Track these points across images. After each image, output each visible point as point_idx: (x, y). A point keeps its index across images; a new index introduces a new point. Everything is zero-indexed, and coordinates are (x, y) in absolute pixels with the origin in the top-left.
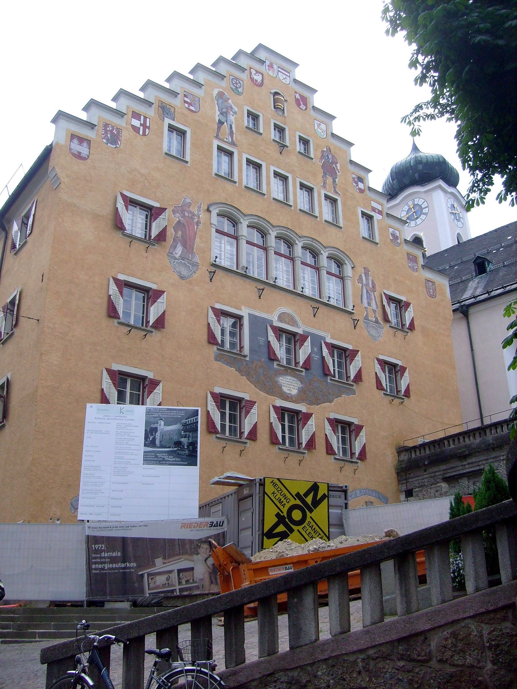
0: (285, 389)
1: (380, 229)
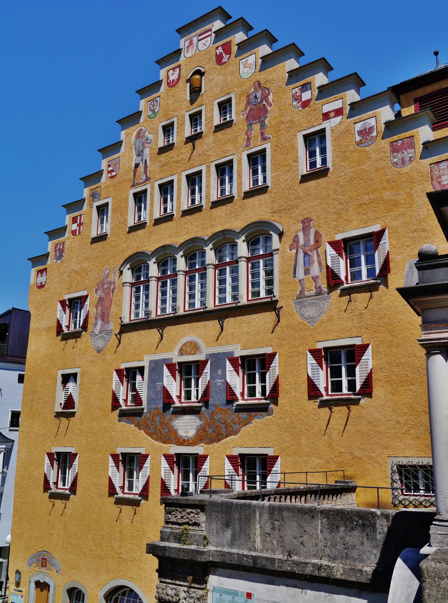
0: (181, 433)
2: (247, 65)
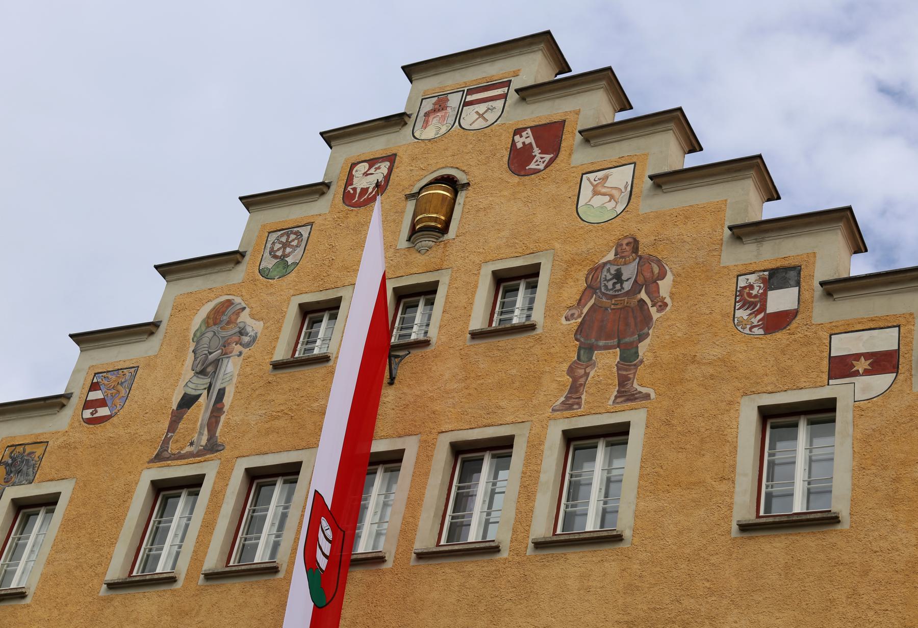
2: (604, 190)
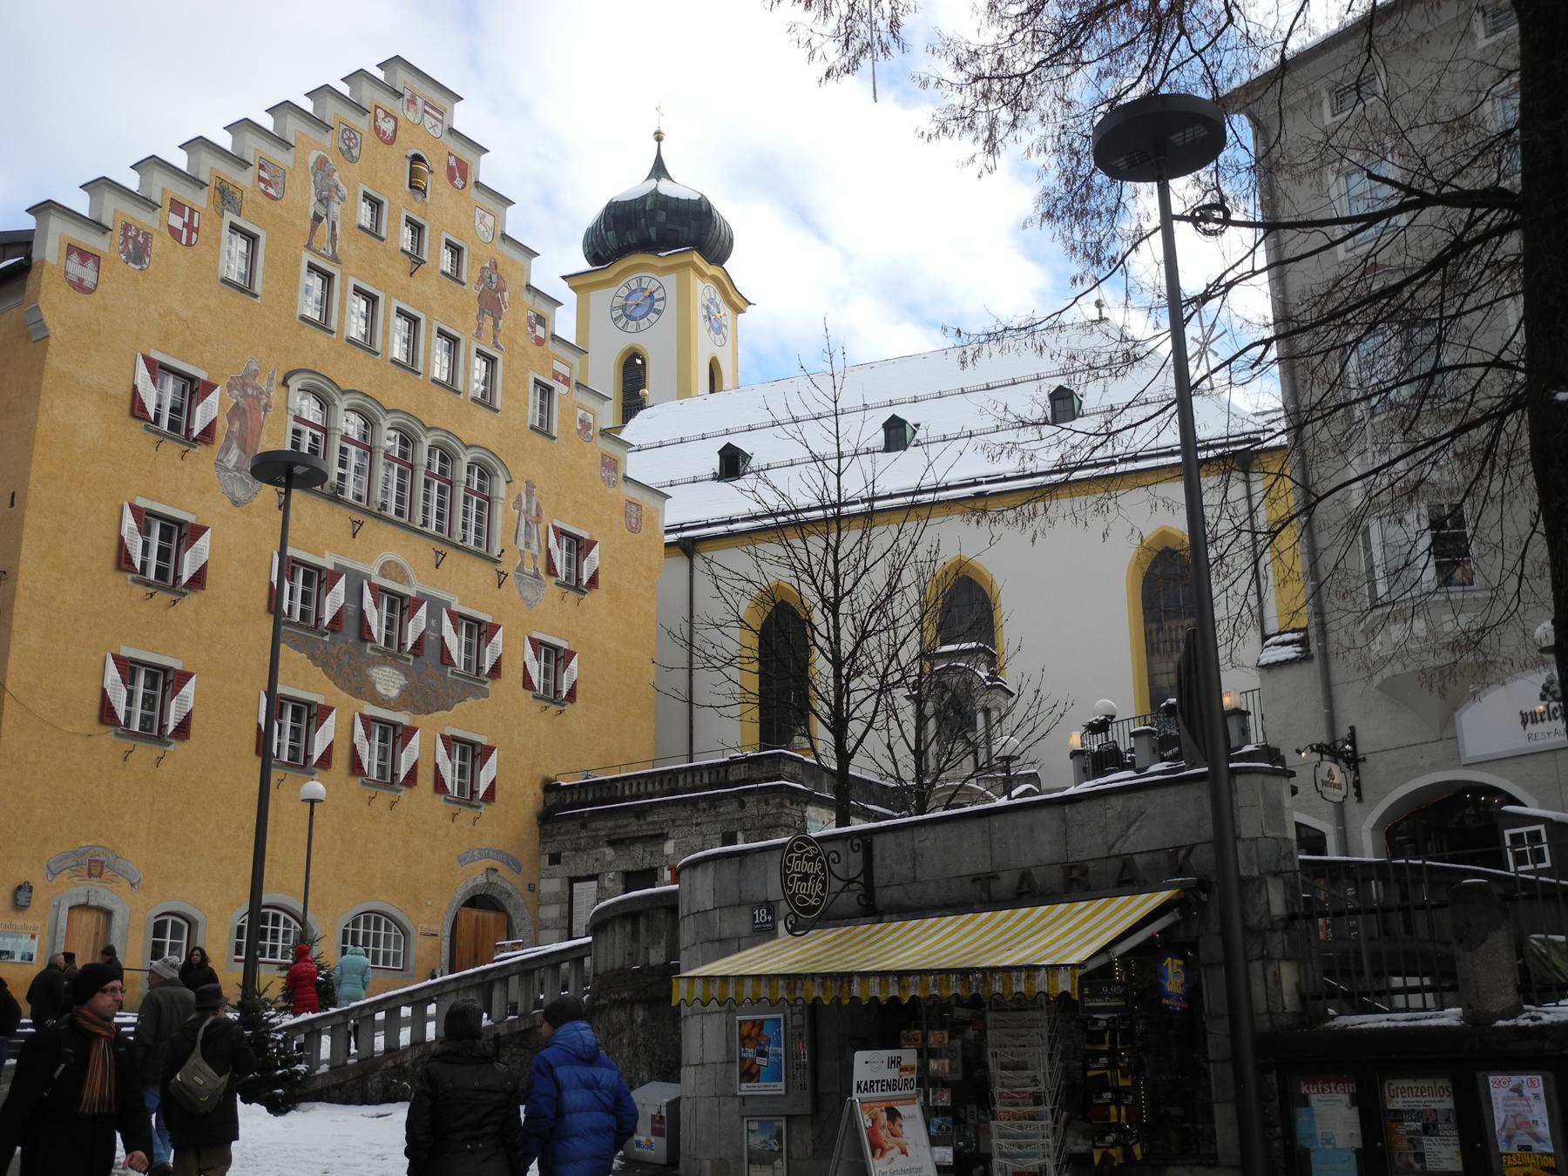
0: (380, 688)
1: (561, 410)
